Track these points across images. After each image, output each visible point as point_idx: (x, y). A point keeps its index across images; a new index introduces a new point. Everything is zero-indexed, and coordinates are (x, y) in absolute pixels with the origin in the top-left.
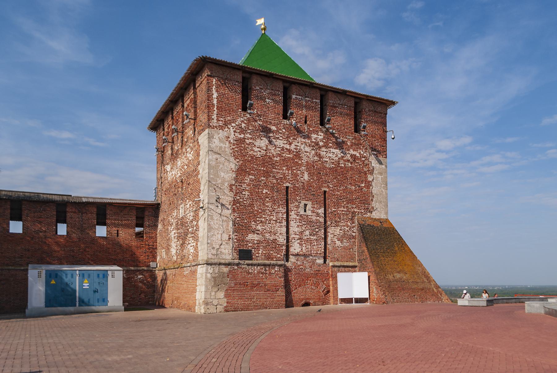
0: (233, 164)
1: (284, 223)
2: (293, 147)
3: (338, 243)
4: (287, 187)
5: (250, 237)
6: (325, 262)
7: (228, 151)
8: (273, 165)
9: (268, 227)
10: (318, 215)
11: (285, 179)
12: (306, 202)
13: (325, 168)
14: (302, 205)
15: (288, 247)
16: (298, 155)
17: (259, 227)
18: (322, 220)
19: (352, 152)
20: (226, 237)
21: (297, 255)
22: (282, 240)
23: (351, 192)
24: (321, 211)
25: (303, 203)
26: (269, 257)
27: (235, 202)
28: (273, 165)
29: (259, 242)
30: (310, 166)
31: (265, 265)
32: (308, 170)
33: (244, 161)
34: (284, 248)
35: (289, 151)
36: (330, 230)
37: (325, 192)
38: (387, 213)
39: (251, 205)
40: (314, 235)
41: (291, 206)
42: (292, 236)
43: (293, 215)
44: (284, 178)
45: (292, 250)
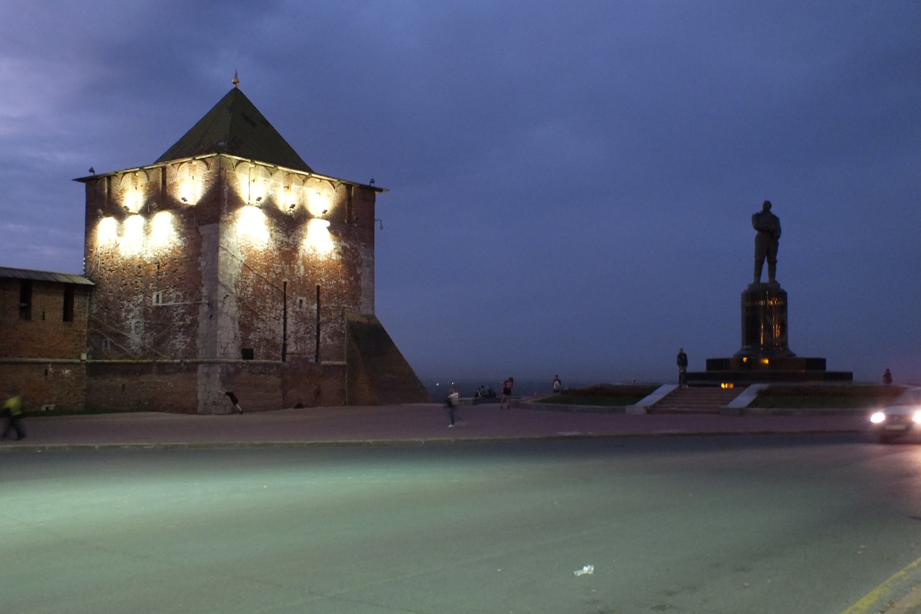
1: (282, 320)
4: (285, 283)
6: (317, 360)
12: (302, 298)
15: (285, 346)
17: (260, 325)
18: (315, 317)
20: (232, 334)
21: (293, 353)
24: (315, 307)
25: (299, 298)
26: (268, 357)
29: (261, 340)
31: (265, 365)
34: (281, 346)
36: (323, 329)
37: (318, 287)
38: (373, 308)
40: (308, 333)
41: (288, 302)
42: (288, 332)
43: (289, 310)
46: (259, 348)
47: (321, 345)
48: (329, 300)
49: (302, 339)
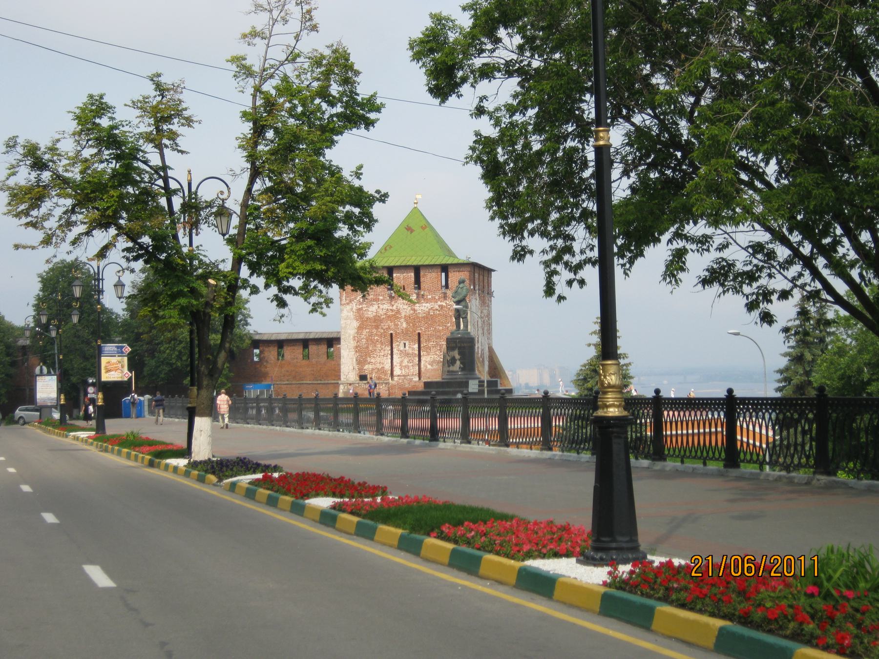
0: (356, 324)
1: (389, 357)
2: (394, 308)
3: (429, 367)
4: (391, 334)
5: (366, 367)
6: (420, 379)
7: (352, 317)
8: (381, 321)
9: (378, 360)
10: (413, 349)
11: (389, 328)
13: (418, 317)
14: (402, 345)
16: (398, 312)
17: (373, 360)
18: (417, 352)
19: (439, 303)
22: (388, 367)
23: (439, 331)
24: (417, 346)
27: (357, 347)
28: (381, 321)
29: (373, 369)
30: (408, 319)
32: (406, 320)
33: (363, 321)
35: (392, 310)
36: (423, 359)
37: (419, 334)
39: (367, 347)
42: (395, 363)
43: (395, 350)
44: (389, 328)
45: (395, 373)
46: (371, 373)
47: (423, 370)
48: (429, 340)
49: (407, 367)
